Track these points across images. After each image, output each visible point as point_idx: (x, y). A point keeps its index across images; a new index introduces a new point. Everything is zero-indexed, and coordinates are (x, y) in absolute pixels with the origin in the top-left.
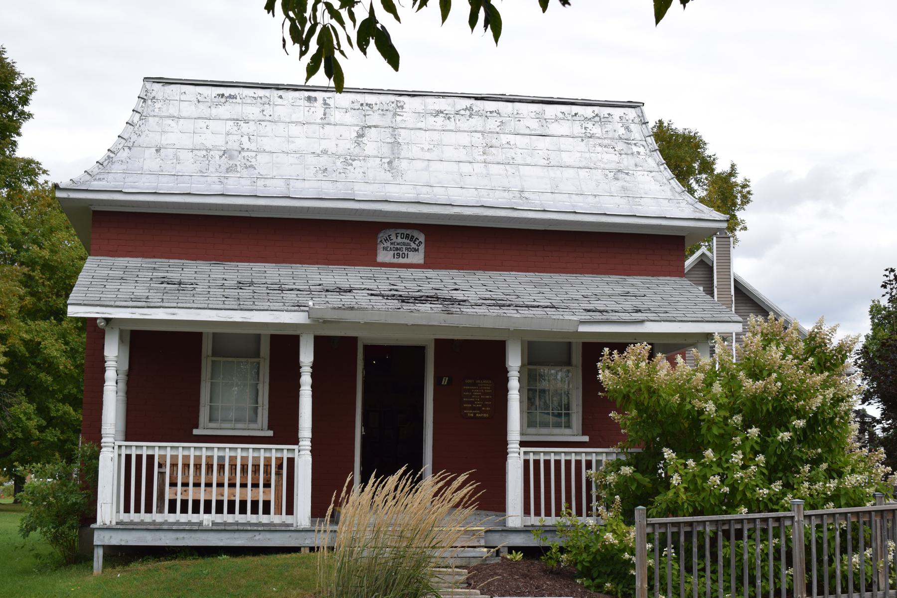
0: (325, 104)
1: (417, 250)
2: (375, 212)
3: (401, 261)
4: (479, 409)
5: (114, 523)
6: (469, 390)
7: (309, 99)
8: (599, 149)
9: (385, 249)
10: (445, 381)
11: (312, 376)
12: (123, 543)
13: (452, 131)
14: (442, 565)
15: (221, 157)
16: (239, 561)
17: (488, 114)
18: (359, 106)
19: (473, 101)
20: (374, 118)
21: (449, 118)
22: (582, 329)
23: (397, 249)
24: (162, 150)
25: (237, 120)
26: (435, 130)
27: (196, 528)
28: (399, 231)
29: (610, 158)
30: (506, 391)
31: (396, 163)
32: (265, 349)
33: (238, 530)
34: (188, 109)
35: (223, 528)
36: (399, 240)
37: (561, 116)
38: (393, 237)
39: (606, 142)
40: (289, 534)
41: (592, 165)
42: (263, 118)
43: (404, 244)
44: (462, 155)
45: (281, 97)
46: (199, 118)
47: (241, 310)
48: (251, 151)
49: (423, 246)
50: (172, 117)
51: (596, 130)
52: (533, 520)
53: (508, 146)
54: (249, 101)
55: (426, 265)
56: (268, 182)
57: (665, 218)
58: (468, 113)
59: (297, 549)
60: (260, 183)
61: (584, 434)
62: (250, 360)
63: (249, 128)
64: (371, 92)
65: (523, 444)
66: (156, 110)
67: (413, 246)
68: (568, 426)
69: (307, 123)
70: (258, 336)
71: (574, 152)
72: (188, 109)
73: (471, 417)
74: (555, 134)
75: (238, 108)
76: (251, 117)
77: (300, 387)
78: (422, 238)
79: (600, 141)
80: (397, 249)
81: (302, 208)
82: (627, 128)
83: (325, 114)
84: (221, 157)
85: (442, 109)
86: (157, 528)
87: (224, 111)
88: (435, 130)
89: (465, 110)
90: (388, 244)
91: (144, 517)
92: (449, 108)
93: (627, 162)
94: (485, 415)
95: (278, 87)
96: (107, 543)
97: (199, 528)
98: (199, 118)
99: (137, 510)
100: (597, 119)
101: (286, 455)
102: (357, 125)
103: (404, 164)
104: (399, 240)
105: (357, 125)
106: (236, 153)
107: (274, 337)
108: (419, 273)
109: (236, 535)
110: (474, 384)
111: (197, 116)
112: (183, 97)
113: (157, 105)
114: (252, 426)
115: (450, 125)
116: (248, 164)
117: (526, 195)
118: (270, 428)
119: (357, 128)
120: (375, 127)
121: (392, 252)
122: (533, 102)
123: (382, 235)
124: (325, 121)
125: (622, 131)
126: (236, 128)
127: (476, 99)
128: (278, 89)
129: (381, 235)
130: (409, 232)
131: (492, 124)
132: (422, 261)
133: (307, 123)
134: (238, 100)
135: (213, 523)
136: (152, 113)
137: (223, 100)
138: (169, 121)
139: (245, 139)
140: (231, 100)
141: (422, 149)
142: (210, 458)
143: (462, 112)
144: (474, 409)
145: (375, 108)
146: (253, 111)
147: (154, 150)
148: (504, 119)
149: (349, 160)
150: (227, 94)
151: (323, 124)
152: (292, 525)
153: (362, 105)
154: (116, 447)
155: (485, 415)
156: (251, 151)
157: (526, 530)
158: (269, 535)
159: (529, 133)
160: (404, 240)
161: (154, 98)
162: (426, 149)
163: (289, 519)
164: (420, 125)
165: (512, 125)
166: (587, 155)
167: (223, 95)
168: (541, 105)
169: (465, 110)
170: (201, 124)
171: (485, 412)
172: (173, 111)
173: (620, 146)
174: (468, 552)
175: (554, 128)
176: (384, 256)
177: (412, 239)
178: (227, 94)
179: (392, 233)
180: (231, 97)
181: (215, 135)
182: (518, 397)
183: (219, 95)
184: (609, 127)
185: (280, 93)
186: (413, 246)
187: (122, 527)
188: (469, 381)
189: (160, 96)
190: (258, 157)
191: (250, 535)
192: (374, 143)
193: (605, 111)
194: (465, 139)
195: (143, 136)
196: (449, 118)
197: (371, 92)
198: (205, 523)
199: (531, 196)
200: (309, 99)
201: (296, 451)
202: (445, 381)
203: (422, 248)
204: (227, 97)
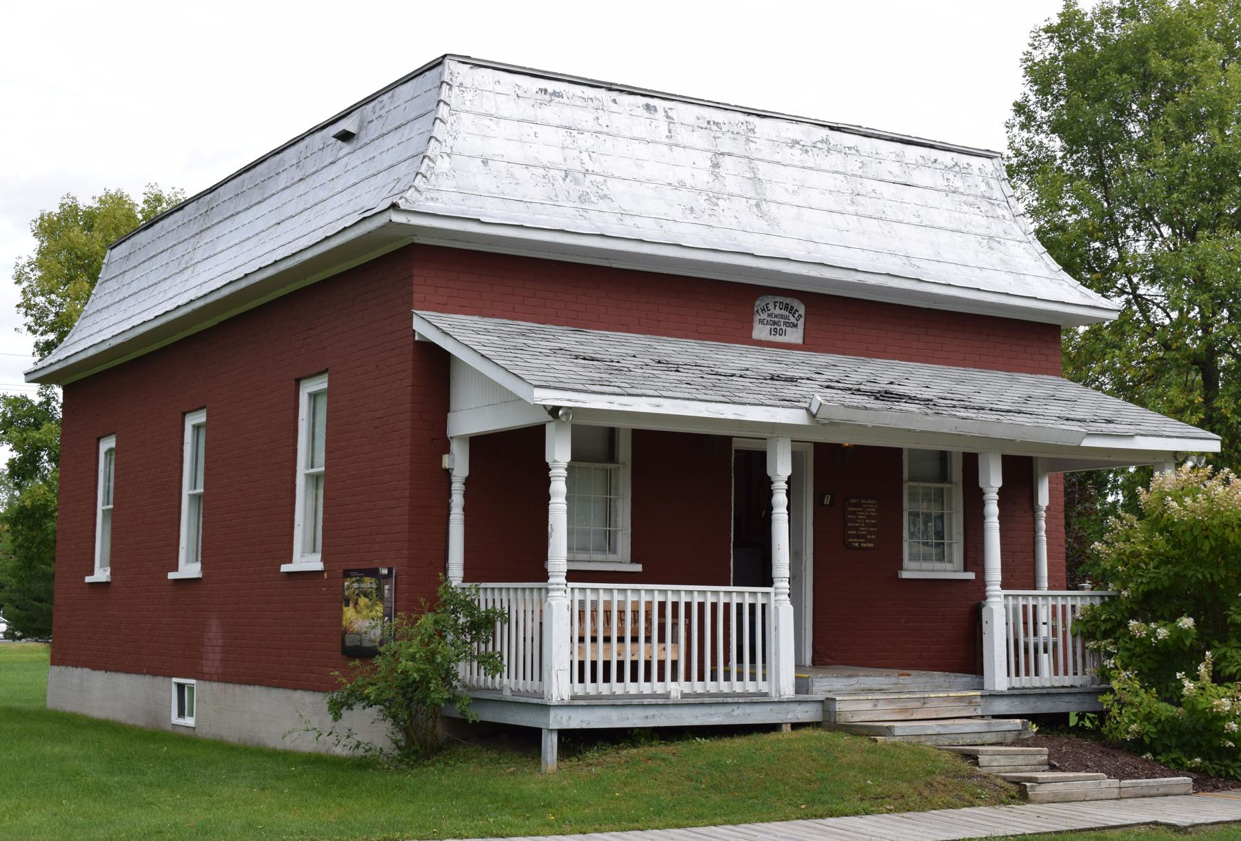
0: (668, 117)
1: (795, 326)
2: (778, 273)
3: (778, 339)
4: (864, 536)
5: (566, 698)
6: (854, 513)
7: (648, 107)
8: (965, 208)
9: (761, 321)
10: (827, 501)
11: (999, 505)
12: (585, 726)
13: (811, 169)
14: (979, 741)
15: (564, 179)
16: (727, 743)
17: (847, 151)
18: (705, 125)
19: (827, 131)
20: (726, 144)
21: (807, 151)
22: (1088, 443)
23: (775, 323)
24: (490, 163)
25: (569, 128)
26: (794, 166)
27: (660, 701)
28: (779, 299)
29: (977, 221)
30: (770, 508)
31: (764, 206)
32: (625, 450)
33: (703, 704)
34: (507, 107)
35: (611, 702)
36: (778, 311)
37: (921, 161)
38: (771, 307)
39: (971, 199)
40: (769, 707)
41: (964, 229)
42: (598, 128)
43: (782, 316)
44: (829, 202)
45: (614, 101)
46: (523, 121)
47: (734, 403)
48: (597, 174)
49: (802, 320)
50: (490, 116)
51: (958, 183)
52: (1016, 682)
53: (873, 195)
54: (579, 103)
55: (806, 346)
56: (638, 221)
57: (1063, 303)
58: (824, 146)
59: (775, 727)
60: (628, 221)
61: (966, 570)
62: (600, 466)
63: (586, 141)
64: (718, 106)
65: (572, 576)
66: (468, 103)
67: (792, 320)
68: (941, 558)
69: (653, 142)
70: (612, 433)
71: (943, 210)
72: (507, 107)
73: (855, 548)
74: (920, 184)
75: (568, 111)
76: (585, 126)
77: (549, 498)
78: (802, 310)
79: (964, 198)
80: (775, 323)
81: (779, 273)
82: (988, 184)
83: (670, 131)
84: (564, 179)
85: (798, 139)
86: (720, 700)
87: (551, 113)
88: (794, 166)
89: (822, 141)
90: (764, 316)
91: (711, 686)
92: (805, 138)
93: (996, 229)
94: (871, 545)
95: (610, 87)
96: (565, 726)
97: (664, 702)
98: (523, 121)
99: (701, 678)
100: (957, 169)
101: (760, 600)
102: (709, 151)
103: (773, 209)
104: (778, 311)
105: (709, 151)
106: (581, 176)
107: (637, 434)
108: (799, 355)
109: (713, 710)
110: (858, 505)
111: (520, 118)
112: (498, 88)
113: (468, 96)
114: (612, 557)
115: (809, 161)
116: (601, 193)
117: (914, 261)
118: (634, 559)
119: (710, 155)
120: (730, 155)
121: (769, 327)
122: (892, 140)
123: (759, 304)
124: (672, 141)
125: (983, 187)
126: (570, 140)
127: (831, 128)
128: (610, 90)
129: (757, 303)
130: (788, 300)
131: (853, 165)
132: (800, 341)
133: (653, 142)
134: (565, 100)
135: (684, 696)
136: (463, 108)
137: (547, 97)
138: (486, 121)
139: (585, 156)
140: (557, 99)
141: (787, 190)
142: (636, 604)
143: (819, 145)
144: (858, 536)
145: (725, 129)
146: (585, 118)
147: (479, 161)
148: (866, 160)
149: (714, 198)
150: (550, 91)
151: (670, 145)
152: (766, 695)
153: (709, 122)
154: (569, 590)
155: (871, 545)
156: (597, 174)
157: (1012, 694)
158: (748, 709)
159: (893, 180)
160: (783, 312)
161: (461, 84)
162: (791, 190)
163: (763, 686)
164: (777, 158)
165: (873, 169)
166: (956, 215)
167: (546, 91)
168: (899, 144)
169: (822, 141)
170: (528, 129)
171: (870, 541)
172: (488, 106)
173: (985, 206)
174: (1001, 725)
175: (918, 177)
176: (760, 332)
177: (792, 310)
178: (550, 91)
179: (770, 300)
180: (555, 94)
181: (548, 147)
182: (565, 507)
183: (541, 90)
184: (970, 180)
185: (614, 95)
186: (792, 320)
187: (575, 703)
188: (853, 501)
189: (467, 82)
190: (609, 183)
191: (727, 709)
192: (733, 175)
193: (964, 159)
194: (829, 181)
195: (460, 139)
196: (807, 151)
197: (718, 106)
198: (673, 694)
199: (922, 264)
200: (648, 107)
201: (773, 595)
202: (827, 501)
203: (801, 323)
204: (551, 95)
